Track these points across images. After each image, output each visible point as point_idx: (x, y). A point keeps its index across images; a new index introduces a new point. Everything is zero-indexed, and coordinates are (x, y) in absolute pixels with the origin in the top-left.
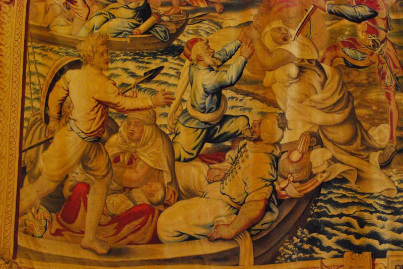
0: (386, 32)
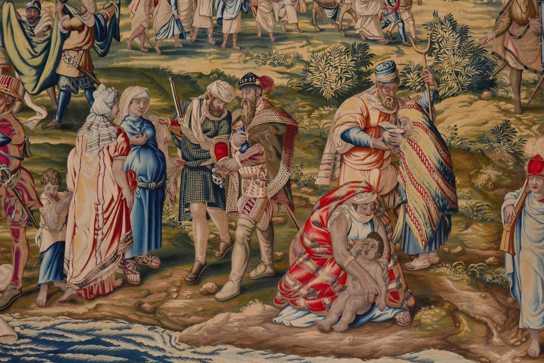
0: (23, 159)
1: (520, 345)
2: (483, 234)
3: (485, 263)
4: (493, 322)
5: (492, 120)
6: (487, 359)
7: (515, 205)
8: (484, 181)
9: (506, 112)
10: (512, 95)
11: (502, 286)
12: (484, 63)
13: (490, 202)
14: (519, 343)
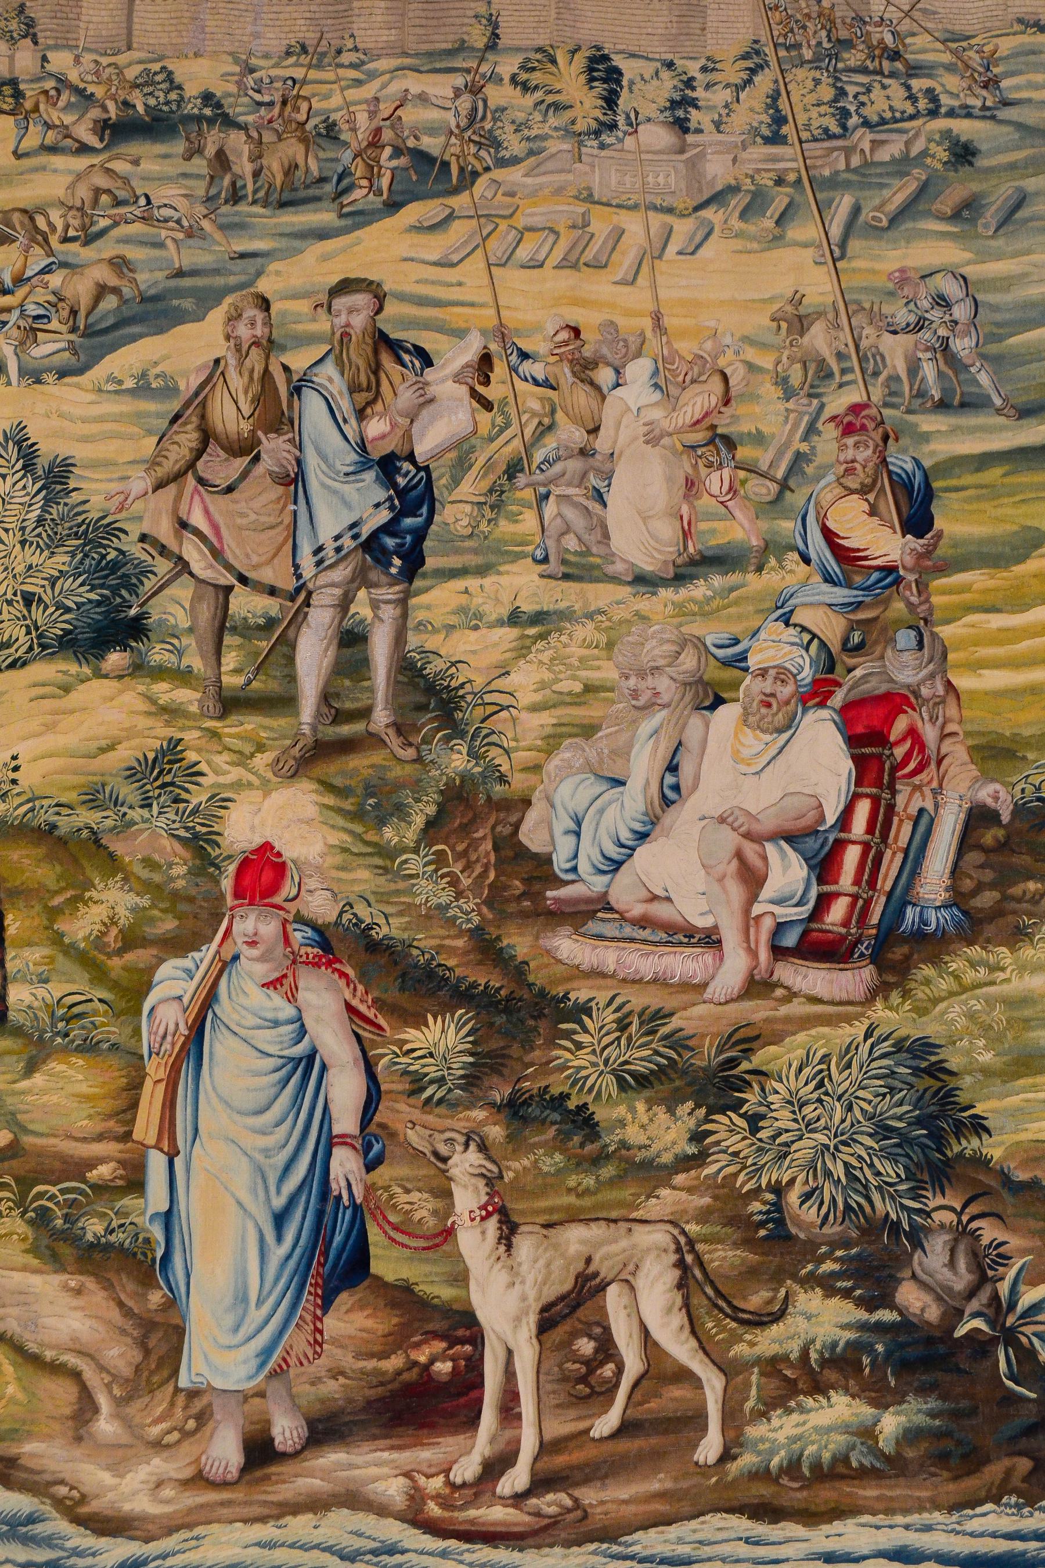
1: (178, 1442)
2: (84, 1088)
3: (84, 1181)
4: (102, 1368)
5: (128, 738)
6: (72, 1488)
7: (186, 1000)
8: (97, 927)
9: (171, 712)
10: (195, 661)
11: (135, 1254)
12: (114, 567)
13: (110, 989)
14: (175, 1436)
